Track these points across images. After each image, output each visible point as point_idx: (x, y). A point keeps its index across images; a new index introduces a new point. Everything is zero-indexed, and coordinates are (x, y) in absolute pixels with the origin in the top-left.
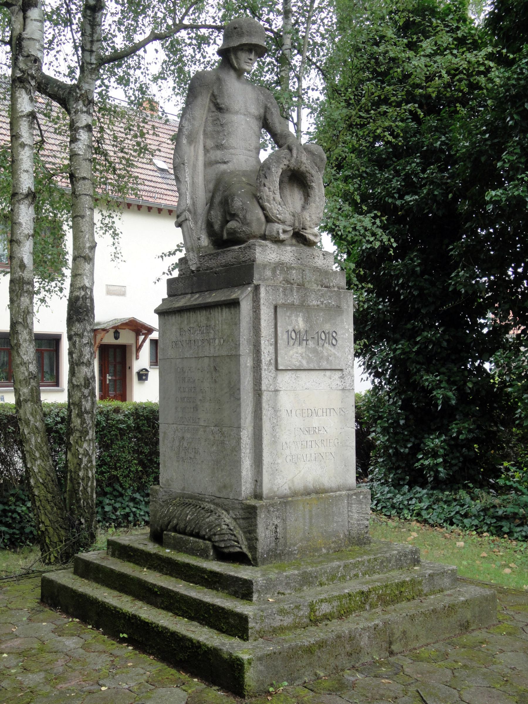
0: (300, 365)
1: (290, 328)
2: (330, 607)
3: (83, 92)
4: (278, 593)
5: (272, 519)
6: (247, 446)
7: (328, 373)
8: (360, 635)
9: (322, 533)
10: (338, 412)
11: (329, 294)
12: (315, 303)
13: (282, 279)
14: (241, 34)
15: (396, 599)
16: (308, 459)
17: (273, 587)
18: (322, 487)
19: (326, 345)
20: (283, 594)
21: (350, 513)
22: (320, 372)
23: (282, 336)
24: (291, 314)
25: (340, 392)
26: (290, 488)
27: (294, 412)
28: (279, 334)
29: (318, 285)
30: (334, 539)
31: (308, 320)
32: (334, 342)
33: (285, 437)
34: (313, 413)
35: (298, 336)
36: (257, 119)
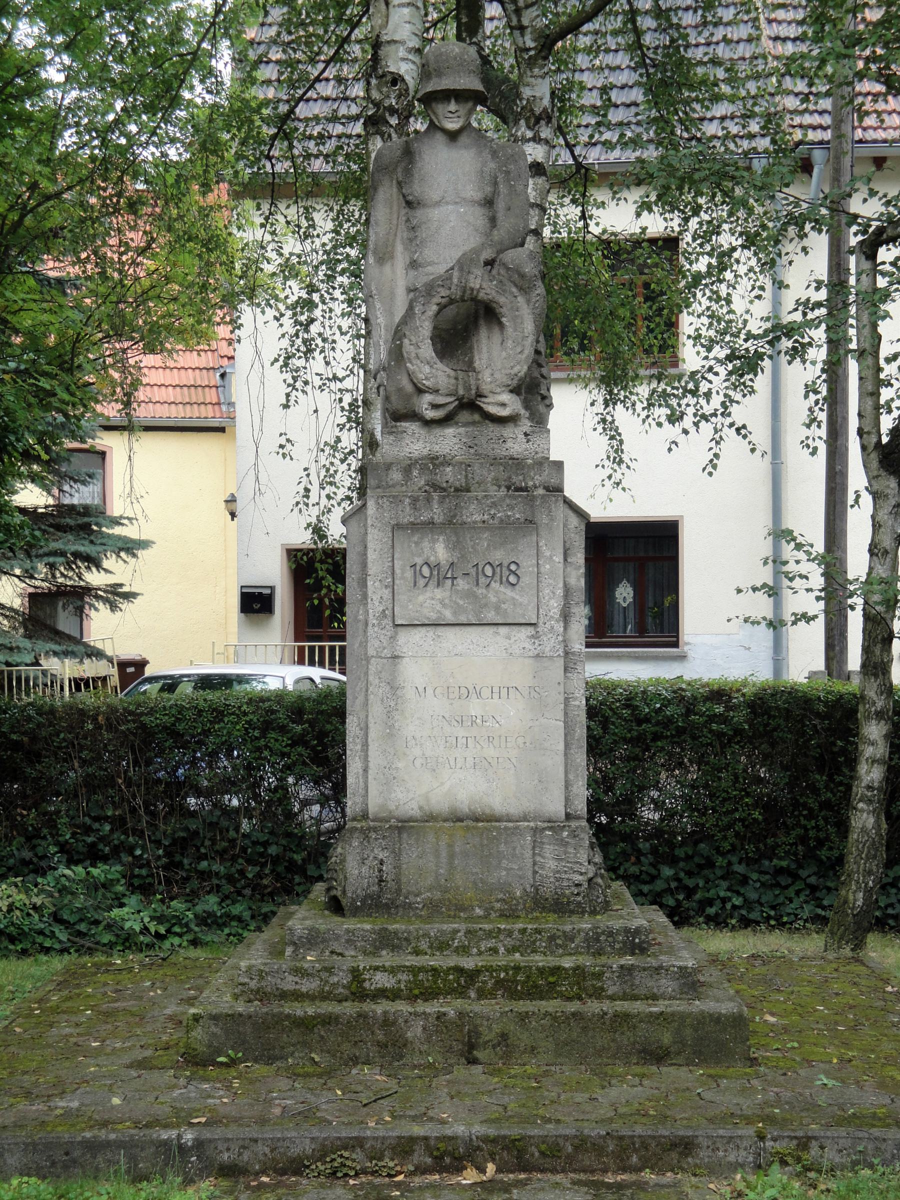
0: (439, 618)
1: (419, 561)
2: (393, 981)
3: (525, 102)
4: (332, 952)
5: (372, 851)
6: (358, 741)
7: (503, 630)
8: (406, 1021)
9: (475, 883)
10: (526, 693)
11: (508, 501)
12: (477, 517)
13: (423, 482)
14: (439, 74)
16: (459, 766)
17: (322, 942)
18: (488, 811)
19: (495, 585)
20: (341, 955)
21: (538, 859)
22: (487, 628)
23: (403, 573)
24: (422, 538)
25: (531, 661)
26: (421, 808)
27: (430, 691)
28: (398, 571)
29: (500, 487)
30: (501, 896)
31: (455, 546)
32: (512, 579)
33: (410, 728)
34: (470, 693)
35: (435, 573)
36: (480, 205)
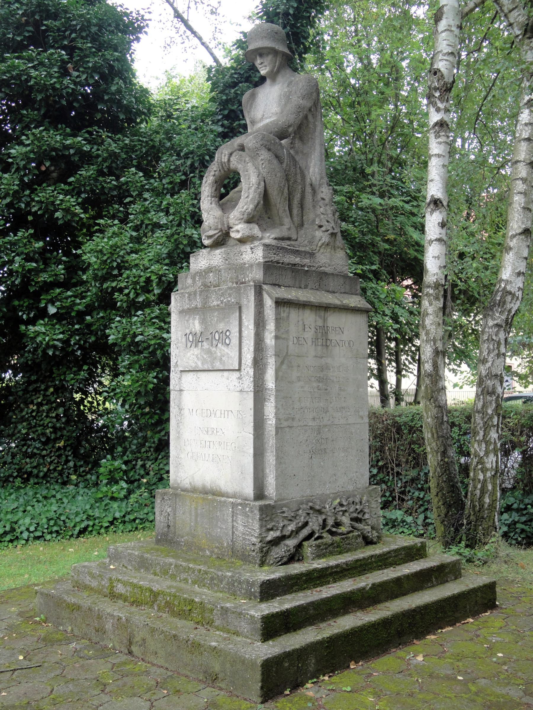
0: (196, 366)
7: (226, 374)
12: (215, 303)
15: (183, 615)
20: (126, 567)
22: (218, 373)
24: (189, 318)
26: (190, 483)
29: (233, 283)
31: (203, 322)
34: (211, 413)
